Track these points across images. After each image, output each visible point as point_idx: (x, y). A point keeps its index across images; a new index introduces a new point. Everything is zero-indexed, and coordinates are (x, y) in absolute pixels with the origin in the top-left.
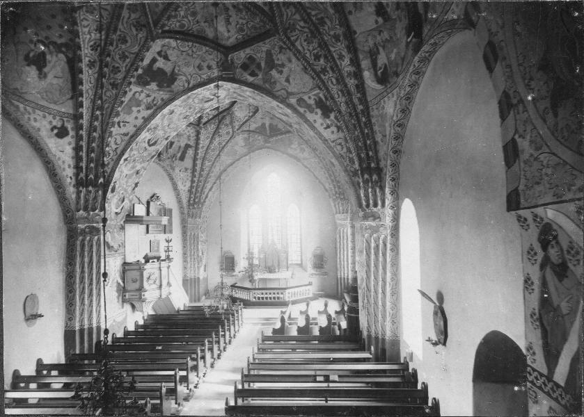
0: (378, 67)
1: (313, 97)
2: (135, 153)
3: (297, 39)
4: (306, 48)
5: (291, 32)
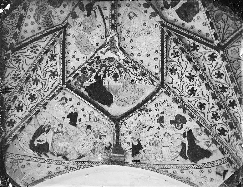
0: (38, 139)
3: (11, 68)
4: (9, 77)
5: (14, 60)
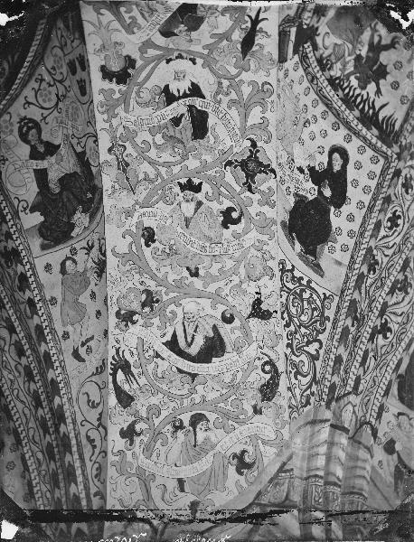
2: (154, 400)
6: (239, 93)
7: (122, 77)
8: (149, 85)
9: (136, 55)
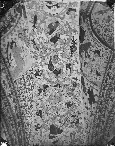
1: (89, 86)
6: (36, 7)
7: (71, 10)
8: (63, 8)
9: (66, 15)
